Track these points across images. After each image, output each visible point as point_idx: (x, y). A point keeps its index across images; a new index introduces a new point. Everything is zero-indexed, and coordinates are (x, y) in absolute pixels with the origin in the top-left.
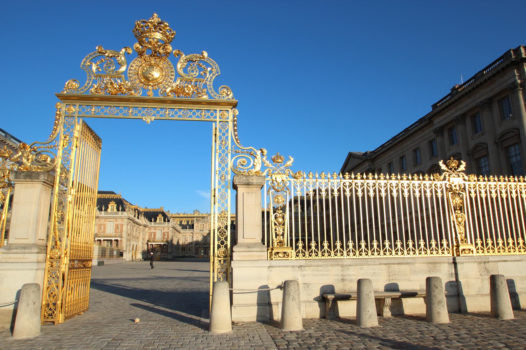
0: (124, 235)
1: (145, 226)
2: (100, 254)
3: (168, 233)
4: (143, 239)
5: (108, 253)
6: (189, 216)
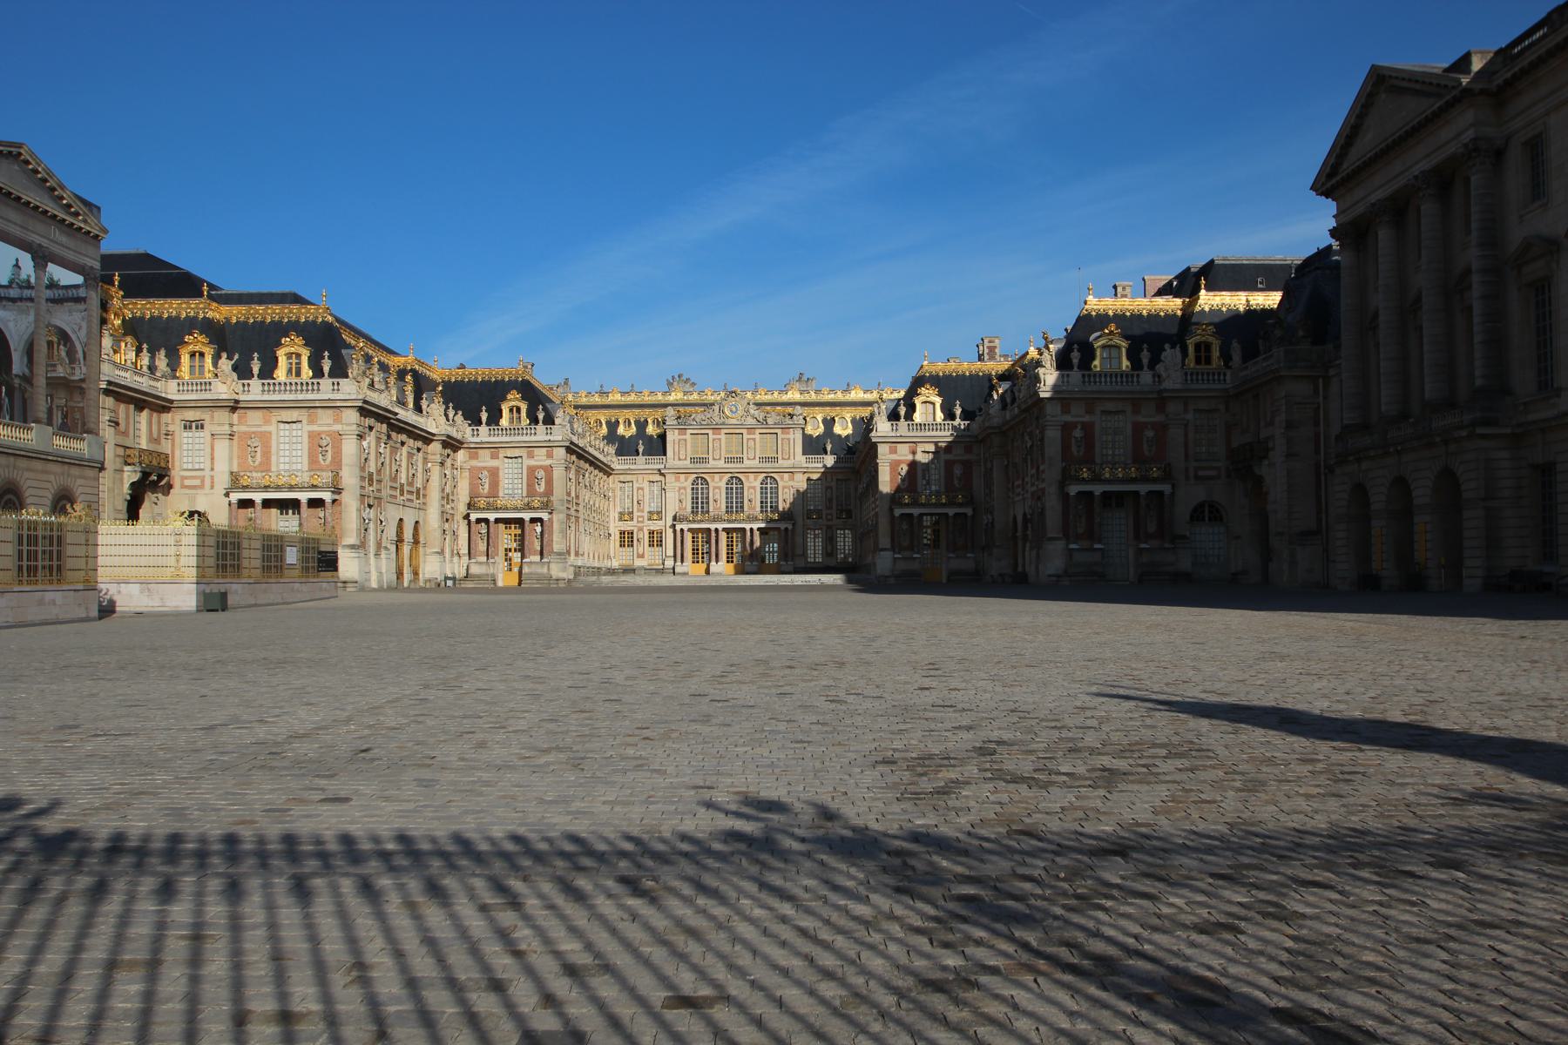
0: (349, 479)
1: (452, 444)
2: (211, 562)
3: (549, 470)
4: (447, 498)
5: (252, 557)
6: (648, 399)
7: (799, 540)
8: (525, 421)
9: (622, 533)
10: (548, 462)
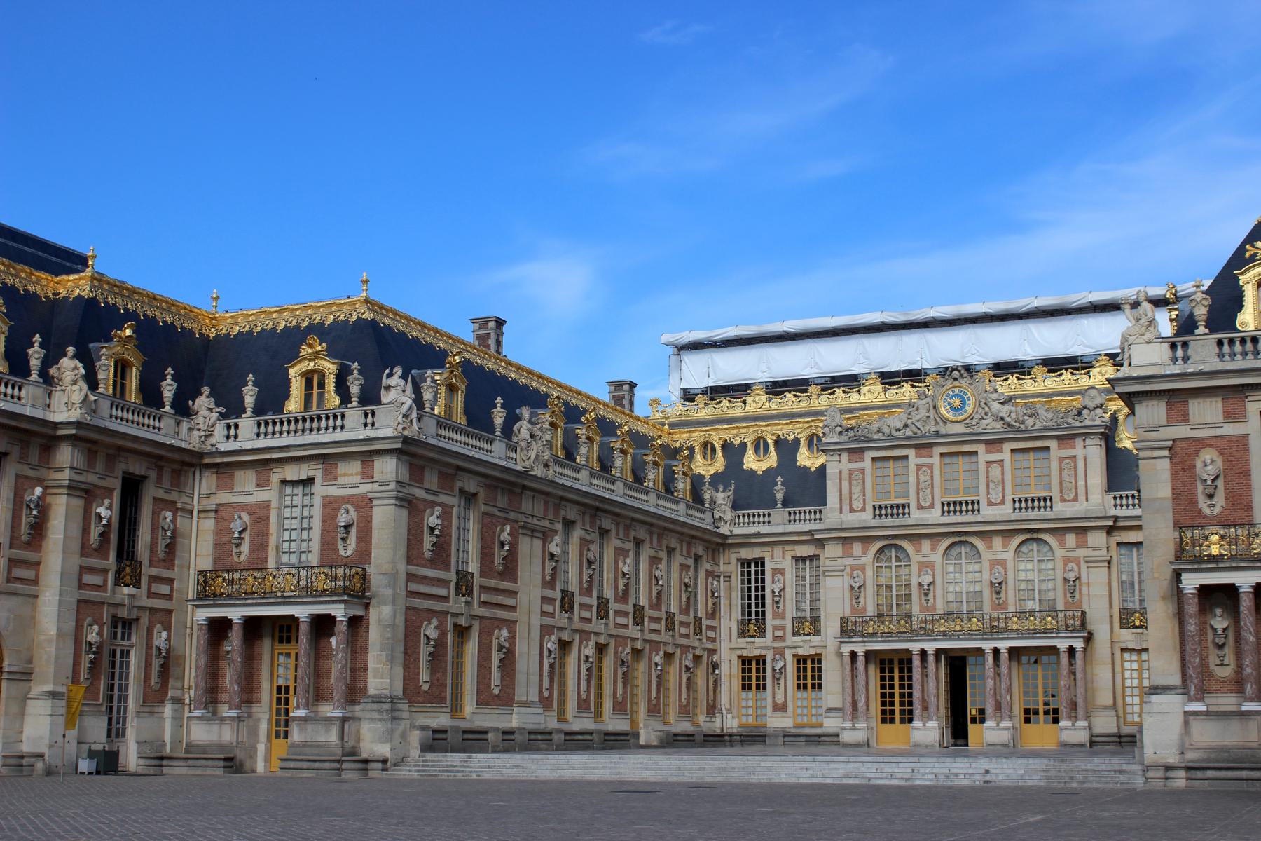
3: (364, 505)
7: (1102, 674)
8: (333, 401)
9: (746, 661)
10: (364, 489)
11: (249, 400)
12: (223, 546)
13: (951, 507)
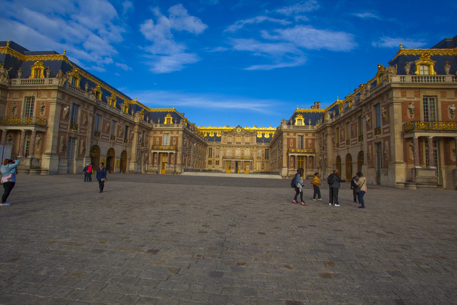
3: (177, 138)
7: (255, 165)
9: (209, 161)
10: (177, 135)
11: (159, 121)
12: (154, 142)
13: (237, 143)
